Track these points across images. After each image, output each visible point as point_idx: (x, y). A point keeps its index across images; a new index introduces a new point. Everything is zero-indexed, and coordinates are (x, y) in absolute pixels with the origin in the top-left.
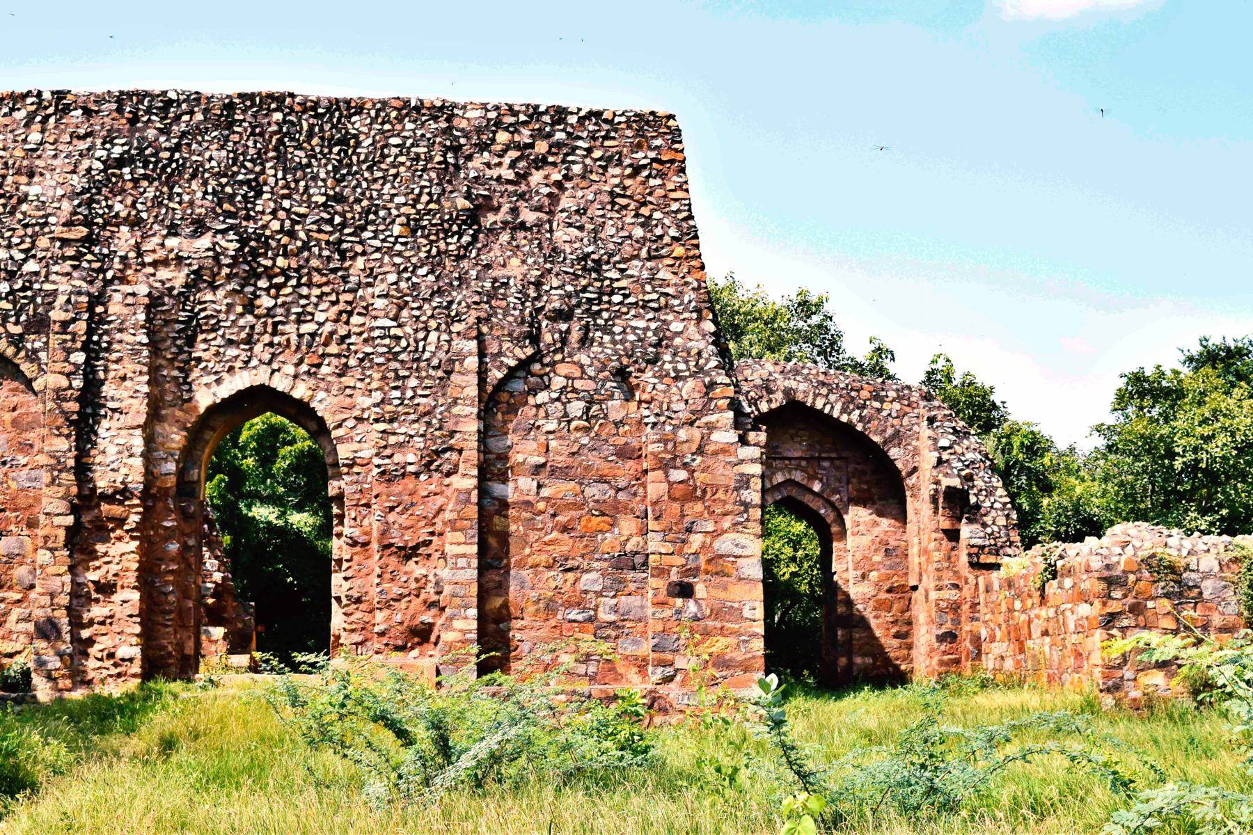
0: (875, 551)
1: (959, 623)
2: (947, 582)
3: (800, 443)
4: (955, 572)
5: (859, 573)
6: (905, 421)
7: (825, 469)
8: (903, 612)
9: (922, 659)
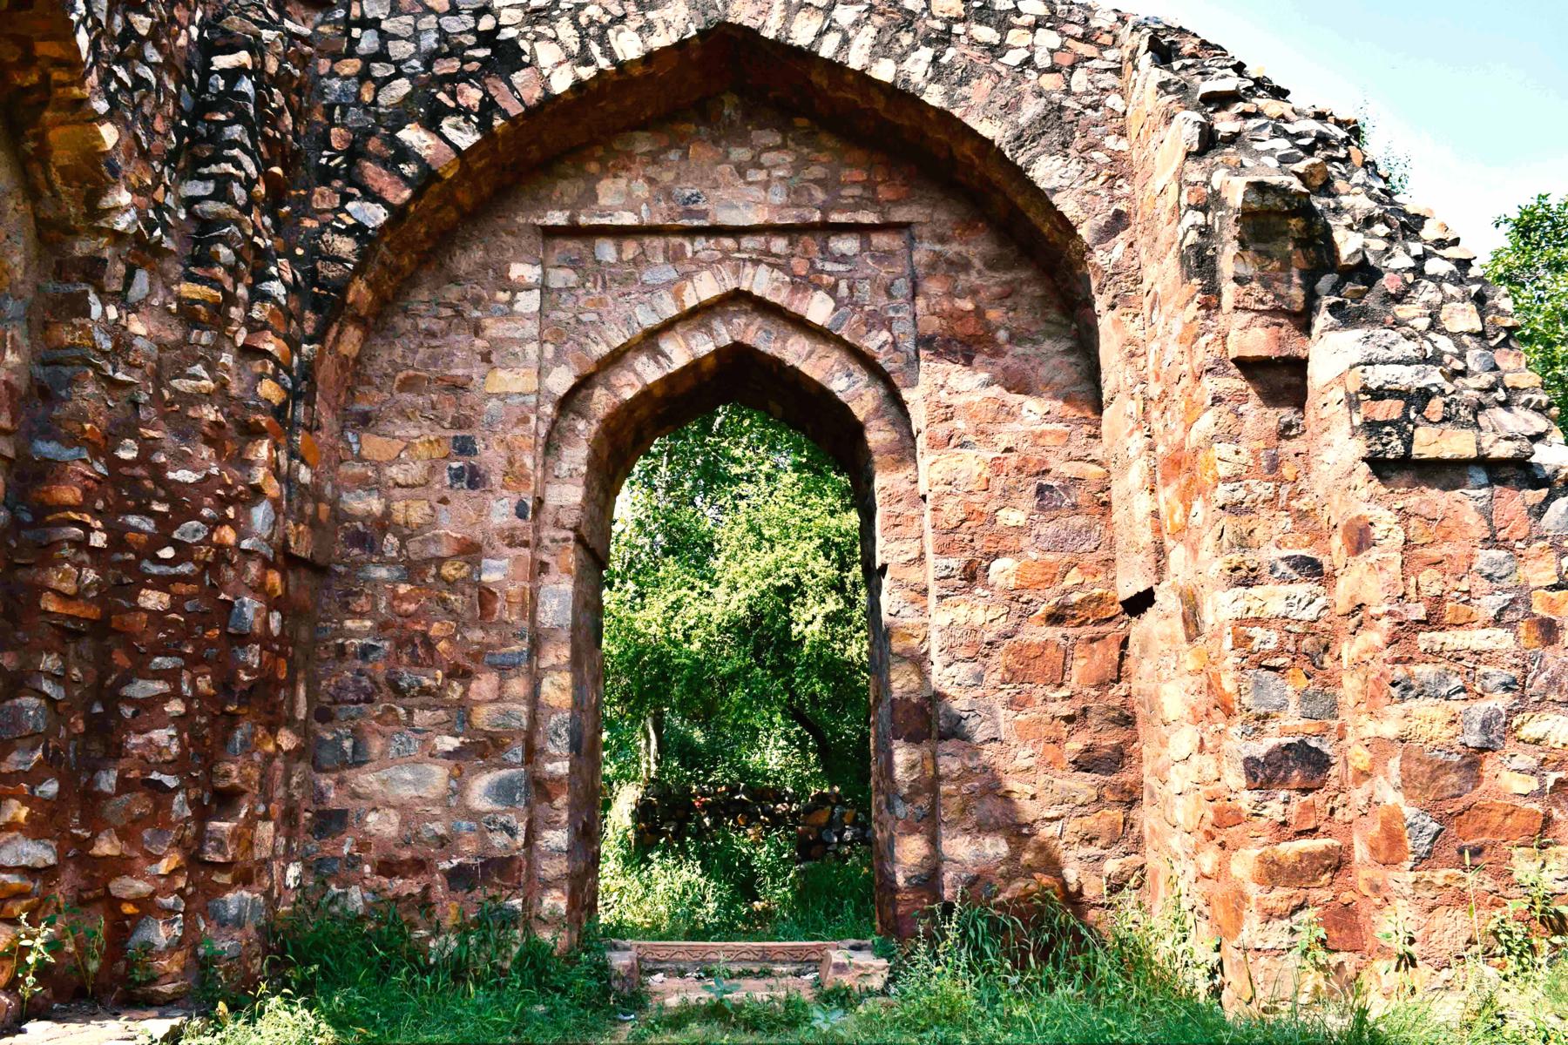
0: (1006, 494)
1: (1333, 710)
2: (1270, 554)
3: (766, 185)
4: (1302, 515)
5: (956, 562)
6: (1080, 80)
7: (843, 258)
8: (1102, 685)
9: (1177, 842)
